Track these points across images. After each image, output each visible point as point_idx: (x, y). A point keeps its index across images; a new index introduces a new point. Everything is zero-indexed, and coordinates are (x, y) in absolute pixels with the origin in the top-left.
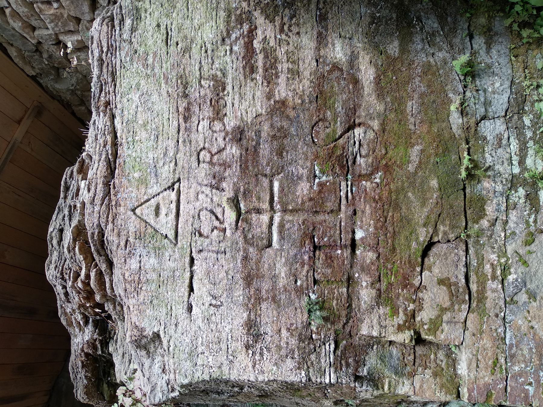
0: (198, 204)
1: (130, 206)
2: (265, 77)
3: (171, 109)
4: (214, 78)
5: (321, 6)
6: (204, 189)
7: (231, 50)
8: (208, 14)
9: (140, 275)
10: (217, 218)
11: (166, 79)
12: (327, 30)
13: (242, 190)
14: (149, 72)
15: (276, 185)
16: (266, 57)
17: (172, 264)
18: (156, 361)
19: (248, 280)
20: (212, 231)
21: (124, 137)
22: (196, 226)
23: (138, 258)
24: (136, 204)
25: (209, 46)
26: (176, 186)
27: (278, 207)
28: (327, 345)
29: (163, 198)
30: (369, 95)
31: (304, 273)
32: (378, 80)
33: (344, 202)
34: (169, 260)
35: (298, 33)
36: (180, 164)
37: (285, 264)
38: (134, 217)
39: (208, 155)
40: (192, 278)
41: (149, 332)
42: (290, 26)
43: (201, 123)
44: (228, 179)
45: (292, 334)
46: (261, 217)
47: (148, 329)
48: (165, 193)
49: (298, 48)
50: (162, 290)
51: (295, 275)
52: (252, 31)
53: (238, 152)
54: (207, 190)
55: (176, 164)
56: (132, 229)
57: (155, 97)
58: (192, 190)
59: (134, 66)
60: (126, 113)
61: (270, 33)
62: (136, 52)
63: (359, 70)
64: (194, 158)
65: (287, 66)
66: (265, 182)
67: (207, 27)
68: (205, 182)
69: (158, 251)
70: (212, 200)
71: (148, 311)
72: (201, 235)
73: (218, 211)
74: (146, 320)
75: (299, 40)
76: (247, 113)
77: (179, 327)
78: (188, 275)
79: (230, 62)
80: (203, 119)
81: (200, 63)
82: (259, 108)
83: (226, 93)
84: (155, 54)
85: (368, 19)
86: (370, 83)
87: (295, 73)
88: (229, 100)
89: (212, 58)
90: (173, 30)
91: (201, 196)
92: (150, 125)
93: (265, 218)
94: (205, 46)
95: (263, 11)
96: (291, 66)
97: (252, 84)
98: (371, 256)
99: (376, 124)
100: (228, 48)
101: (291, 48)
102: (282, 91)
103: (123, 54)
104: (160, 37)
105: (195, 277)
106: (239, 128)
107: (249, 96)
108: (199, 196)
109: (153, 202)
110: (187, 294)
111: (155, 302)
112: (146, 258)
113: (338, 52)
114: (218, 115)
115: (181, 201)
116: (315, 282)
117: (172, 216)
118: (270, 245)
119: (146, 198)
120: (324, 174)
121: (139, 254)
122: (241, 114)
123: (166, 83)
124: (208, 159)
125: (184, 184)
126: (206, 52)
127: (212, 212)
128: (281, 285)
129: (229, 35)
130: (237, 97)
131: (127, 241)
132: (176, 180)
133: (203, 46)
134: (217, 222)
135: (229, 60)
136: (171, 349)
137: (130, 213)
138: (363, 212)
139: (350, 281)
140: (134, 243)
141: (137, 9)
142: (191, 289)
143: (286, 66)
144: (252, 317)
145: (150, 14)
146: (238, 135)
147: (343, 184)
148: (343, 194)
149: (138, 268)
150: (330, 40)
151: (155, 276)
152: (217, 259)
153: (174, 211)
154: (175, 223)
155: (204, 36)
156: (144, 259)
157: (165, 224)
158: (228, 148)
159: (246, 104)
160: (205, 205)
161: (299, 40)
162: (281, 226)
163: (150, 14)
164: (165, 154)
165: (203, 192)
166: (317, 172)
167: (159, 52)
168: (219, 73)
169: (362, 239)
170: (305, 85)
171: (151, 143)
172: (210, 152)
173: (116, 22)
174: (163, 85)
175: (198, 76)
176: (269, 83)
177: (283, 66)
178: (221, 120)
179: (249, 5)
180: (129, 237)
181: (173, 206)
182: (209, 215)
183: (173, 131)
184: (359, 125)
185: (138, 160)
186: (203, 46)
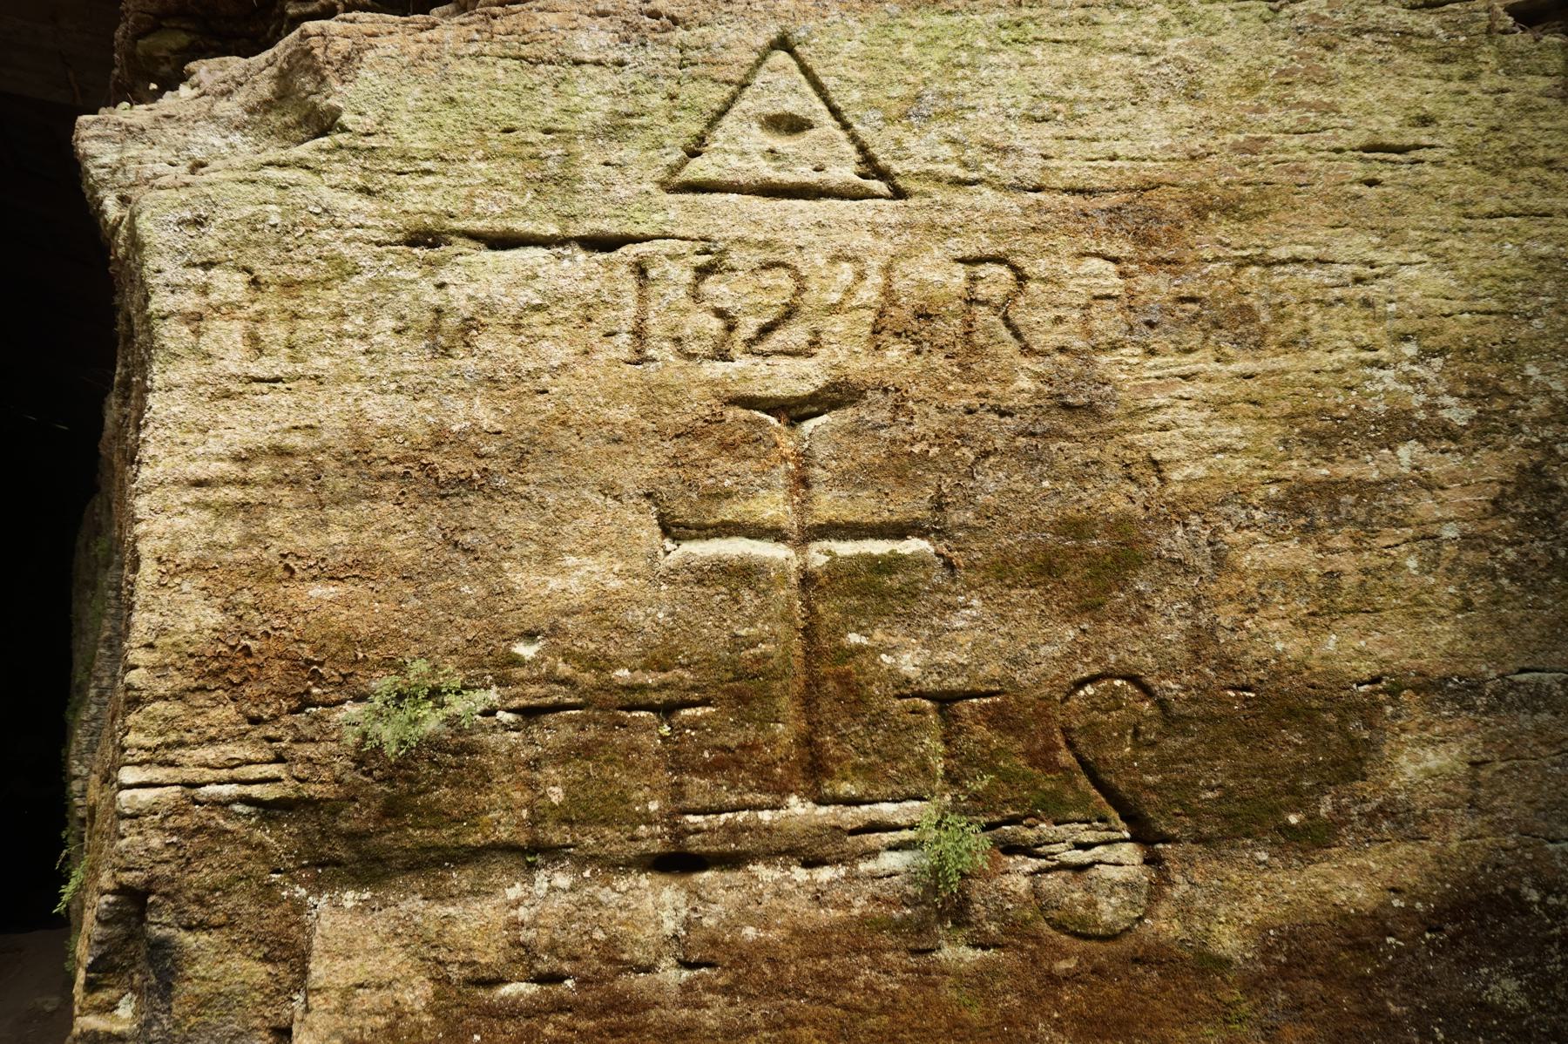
3: (1149, 164)
6: (875, 279)
8: (1488, 282)
9: (550, 62)
10: (766, 330)
11: (1252, 147)
12: (1491, 709)
20: (720, 313)
22: (736, 257)
23: (614, 55)
26: (877, 186)
27: (817, 555)
28: (273, 770)
29: (832, 140)
34: (606, 164)
35: (1467, 605)
36: (961, 198)
38: (761, 41)
42: (1493, 574)
43: (1112, 267)
48: (850, 149)
49: (1417, 609)
54: (869, 293)
55: (958, 182)
56: (717, 34)
59: (1280, 43)
62: (1328, 48)
63: (1358, 849)
64: (987, 246)
65: (1349, 568)
67: (1442, 281)
68: (899, 284)
70: (833, 309)
71: (417, 91)
72: (703, 272)
73: (794, 334)
74: (383, 84)
75: (1443, 611)
76: (1164, 428)
77: (354, 201)
80: (1123, 275)
81: (1321, 261)
82: (1187, 471)
83: (1229, 350)
84: (1331, 109)
86: (1322, 894)
89: (1339, 300)
90: (1418, 167)
91: (846, 271)
92: (1087, 94)
93: (772, 506)
94: (1377, 276)
96: (1349, 582)
97: (1269, 443)
99: (1165, 926)
104: (1389, 127)
108: (846, 265)
109: (813, 106)
113: (1420, 761)
114: (1146, 325)
115: (824, 203)
117: (767, 171)
119: (829, 82)
121: (628, 58)
122: (1157, 408)
123: (1237, 148)
124: (982, 291)
125: (890, 211)
126: (1359, 280)
127: (790, 313)
130: (1216, 389)
132: (900, 182)
133: (1376, 271)
134: (755, 329)
135: (1343, 356)
136: (273, 173)
137: (772, 30)
140: (667, 43)
148: (887, 810)
149: (576, 55)
153: (788, 178)
154: (742, 179)
160: (813, 284)
161: (1443, 611)
162: (746, 573)
164: (990, 147)
165: (861, 276)
167: (1336, 121)
172: (1010, 298)
174: (1229, 138)
175: (1273, 253)
180: (687, 28)
182: (778, 300)
183: (1071, 169)
184: (1152, 860)
186: (1376, 271)
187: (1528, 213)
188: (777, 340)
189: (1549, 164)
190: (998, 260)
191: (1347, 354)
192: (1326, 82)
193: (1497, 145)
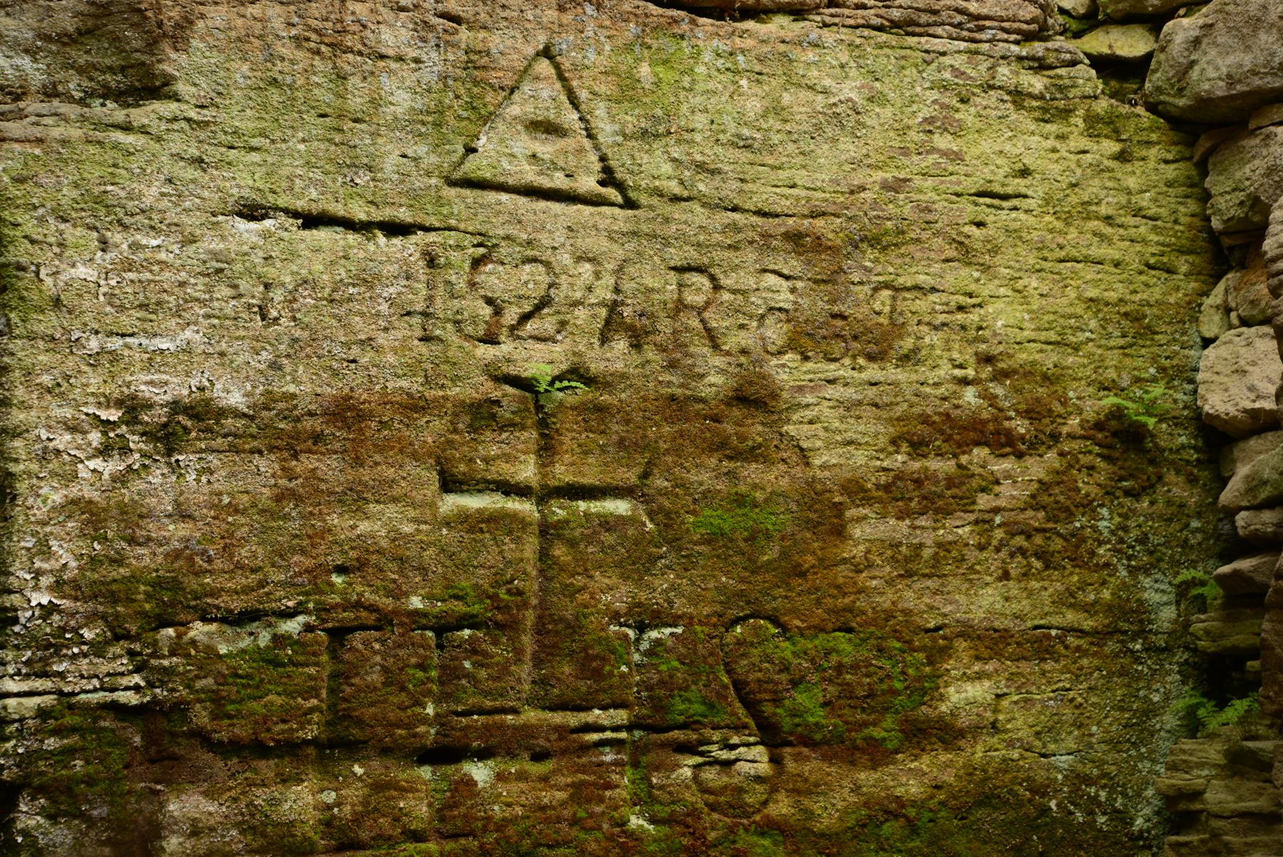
0: (566, 258)
1: (564, 42)
2: (900, 476)
3: (820, 195)
4: (897, 328)
5: (1072, 640)
6: (609, 280)
7: (965, 382)
8: (1052, 317)
9: (360, 53)
10: (525, 318)
13: (605, 398)
14: (914, 136)
15: (621, 507)
16: (950, 482)
17: (391, 163)
18: (25, 62)
19: (345, 412)
20: (489, 301)
21: (749, 43)
22: (504, 249)
23: (413, 53)
24: (566, 65)
25: (973, 317)
26: (612, 193)
27: (558, 510)
28: (137, 679)
30: (856, 789)
31: (369, 597)
32: (894, 809)
33: (573, 719)
34: (404, 156)
36: (676, 211)
37: (396, 537)
38: (530, 51)
39: (699, 299)
40: (349, 225)
41: (173, 62)
43: (786, 284)
44: (636, 358)
45: (177, 555)
46: (532, 459)
47: (183, 59)
48: (593, 157)
50: (316, 127)
51: (361, 565)
52: (1004, 443)
53: (705, 392)
54: (604, 292)
55: (676, 199)
56: (496, 42)
57: (848, 148)
58: (605, 244)
59: (928, 93)
60: (811, 55)
61: (1007, 491)
62: (962, 101)
64: (692, 255)
65: (929, 542)
66: (630, 476)
67: (1019, 313)
68: (627, 286)
69: (432, 121)
70: (576, 304)
71: (245, 68)
72: (477, 263)
73: (546, 323)
74: (215, 58)
75: (988, 579)
76: (811, 422)
77: (191, 173)
78: (360, 212)
79: (939, 374)
80: (793, 290)
81: (934, 290)
82: (825, 458)
83: (861, 361)
84: (957, 157)
85: (1040, 776)
86: (888, 788)
87: (908, 565)
88: (840, 370)
89: (944, 324)
90: (1014, 214)
92: (778, 125)
93: (527, 471)
94: (974, 306)
95: (1060, 478)
96: (927, 553)
97: (882, 441)
98: (419, 810)
100: (970, 373)
101: (972, 555)
102: (869, 529)
103: (959, 61)
104: (997, 175)
105: (352, 238)
106: (774, 396)
107: (854, 430)
108: (588, 266)
109: (570, 118)
110: (300, 205)
111: (275, 96)
112: (410, 79)
116: (339, 634)
117: (530, 175)
118: (450, 484)
119: (583, 95)
120: (649, 653)
121: (425, 58)
122: (808, 406)
123: (886, 186)
124: (690, 298)
126: (961, 308)
127: (544, 302)
128: (334, 520)
129: (1000, 376)
130: (850, 393)
131: (457, 20)
132: (632, 194)
133: (974, 301)
134: (516, 317)
135: (942, 373)
136: (119, 136)
137: (542, 39)
138: (544, 779)
139: (336, 747)
140: (455, 45)
141: (1066, 113)
142: (312, 221)
143: (928, 538)
144: (229, 422)
145: (1054, 150)
146: (753, 398)
147: (621, 716)
149: (384, 51)
150: (990, 667)
151: (356, 102)
152: (408, 314)
153: (546, 183)
154: (511, 181)
155: (999, 305)
156: (405, 71)
157: (506, 151)
158: (718, 361)
159: (834, 423)
161: (988, 579)
163: (1054, 150)
164: (701, 167)
165: (597, 275)
166: (654, 634)
167: (962, 169)
168: (908, 343)
169: (470, 782)
170: (883, 592)
171: (732, 128)
172: (708, 303)
173: (1038, 48)
174: (879, 176)
175: (901, 280)
176: (887, 488)
177: (927, 533)
178: (791, 345)
179: (1071, 436)
180: (470, 29)
181: (558, 181)
182: (536, 292)
183: (763, 195)
184: (775, 760)
185: (686, 81)
186: (974, 301)
187: (1087, 260)
188: (530, 327)
189: (1108, 219)
190: (700, 270)
191: (945, 370)
192: (958, 131)
193: (1074, 199)
